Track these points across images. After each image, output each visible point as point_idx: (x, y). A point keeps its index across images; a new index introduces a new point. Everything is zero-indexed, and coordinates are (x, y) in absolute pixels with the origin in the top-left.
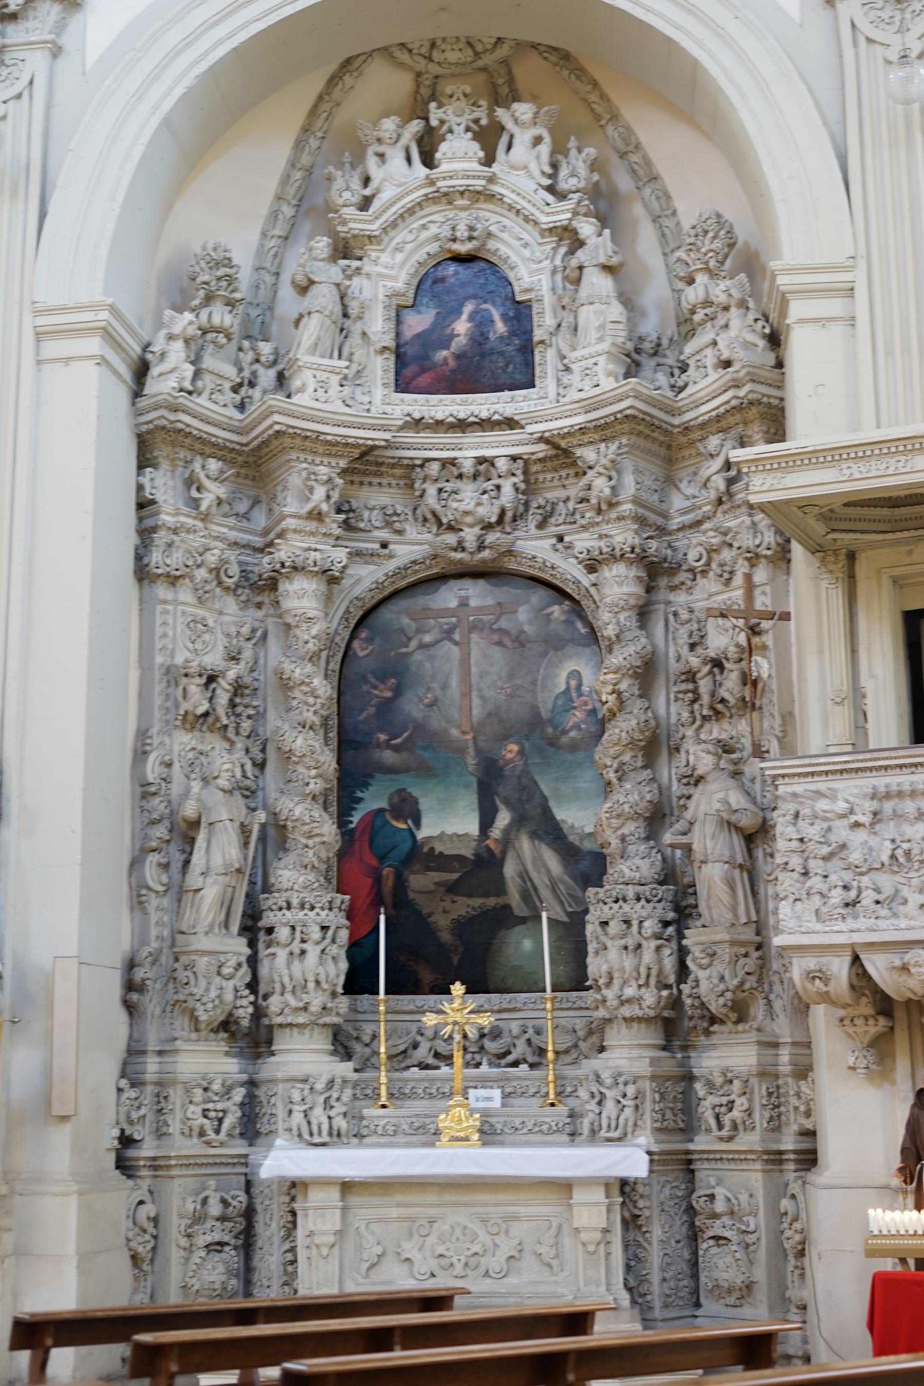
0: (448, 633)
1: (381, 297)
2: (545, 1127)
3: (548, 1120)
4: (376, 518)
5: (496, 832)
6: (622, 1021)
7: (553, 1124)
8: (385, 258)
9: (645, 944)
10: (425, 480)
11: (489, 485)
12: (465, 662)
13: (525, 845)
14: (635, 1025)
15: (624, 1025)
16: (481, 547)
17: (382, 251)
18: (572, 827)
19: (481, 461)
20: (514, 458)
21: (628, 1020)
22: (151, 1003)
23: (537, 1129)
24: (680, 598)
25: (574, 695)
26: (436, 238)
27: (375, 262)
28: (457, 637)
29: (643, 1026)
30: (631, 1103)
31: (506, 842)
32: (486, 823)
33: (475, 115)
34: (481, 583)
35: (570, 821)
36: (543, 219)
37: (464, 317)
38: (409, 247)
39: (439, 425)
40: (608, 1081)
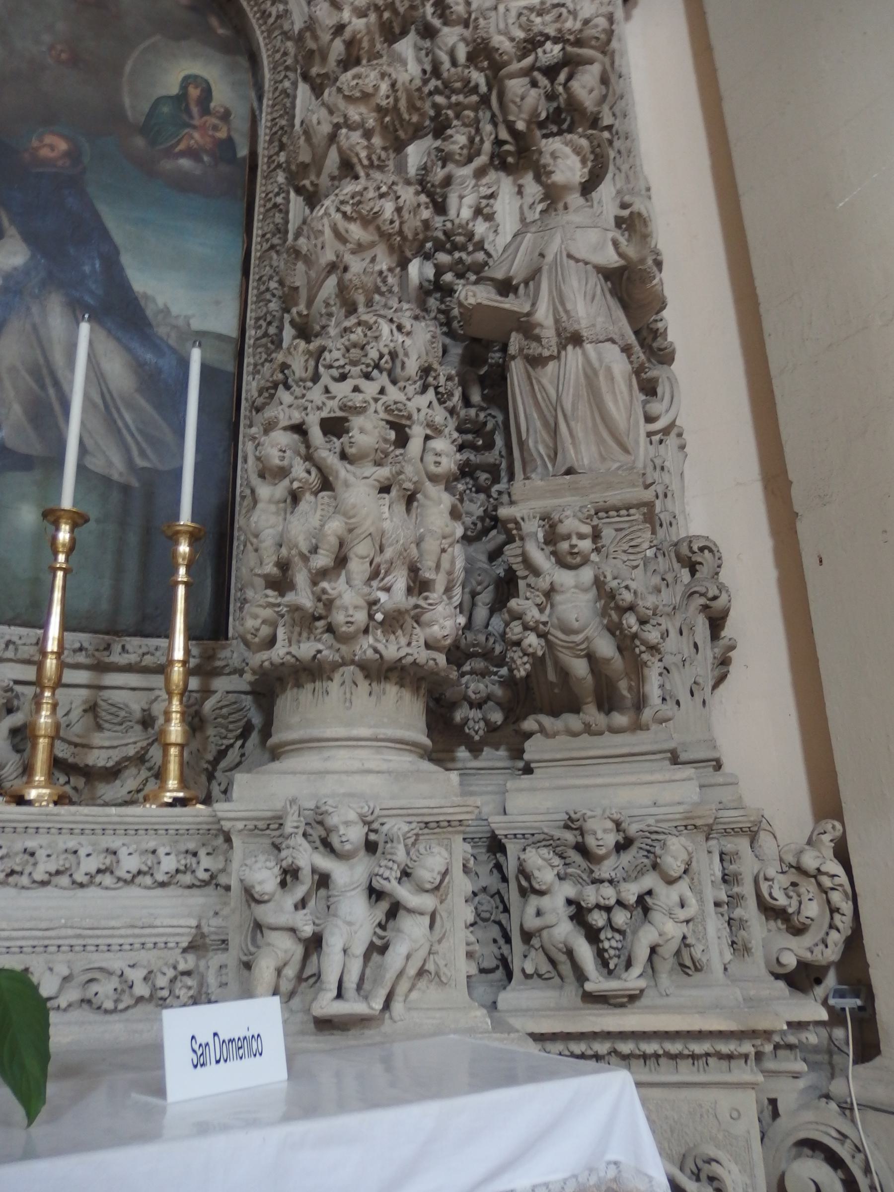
2: (105, 989)
3: (116, 963)
6: (359, 676)
7: (136, 976)
14: (392, 690)
15: (364, 685)
18: (166, 311)
23: (73, 994)
25: (195, 110)
30: (427, 902)
35: (160, 302)
40: (355, 835)
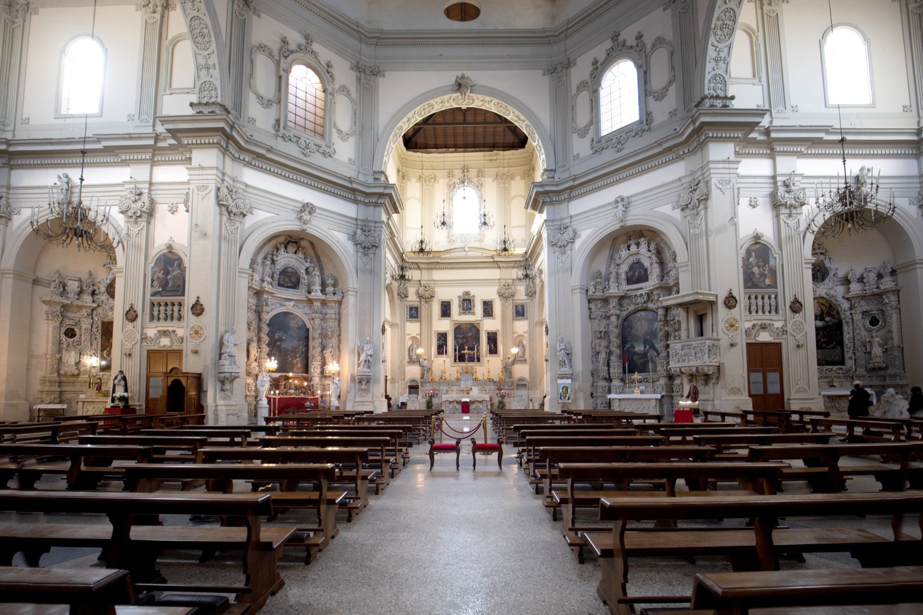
0: (638, 320)
4: (625, 304)
5: (646, 349)
12: (641, 324)
13: (651, 351)
22: (595, 376)
24: (672, 312)
31: (648, 351)
32: (645, 348)
39: (634, 290)
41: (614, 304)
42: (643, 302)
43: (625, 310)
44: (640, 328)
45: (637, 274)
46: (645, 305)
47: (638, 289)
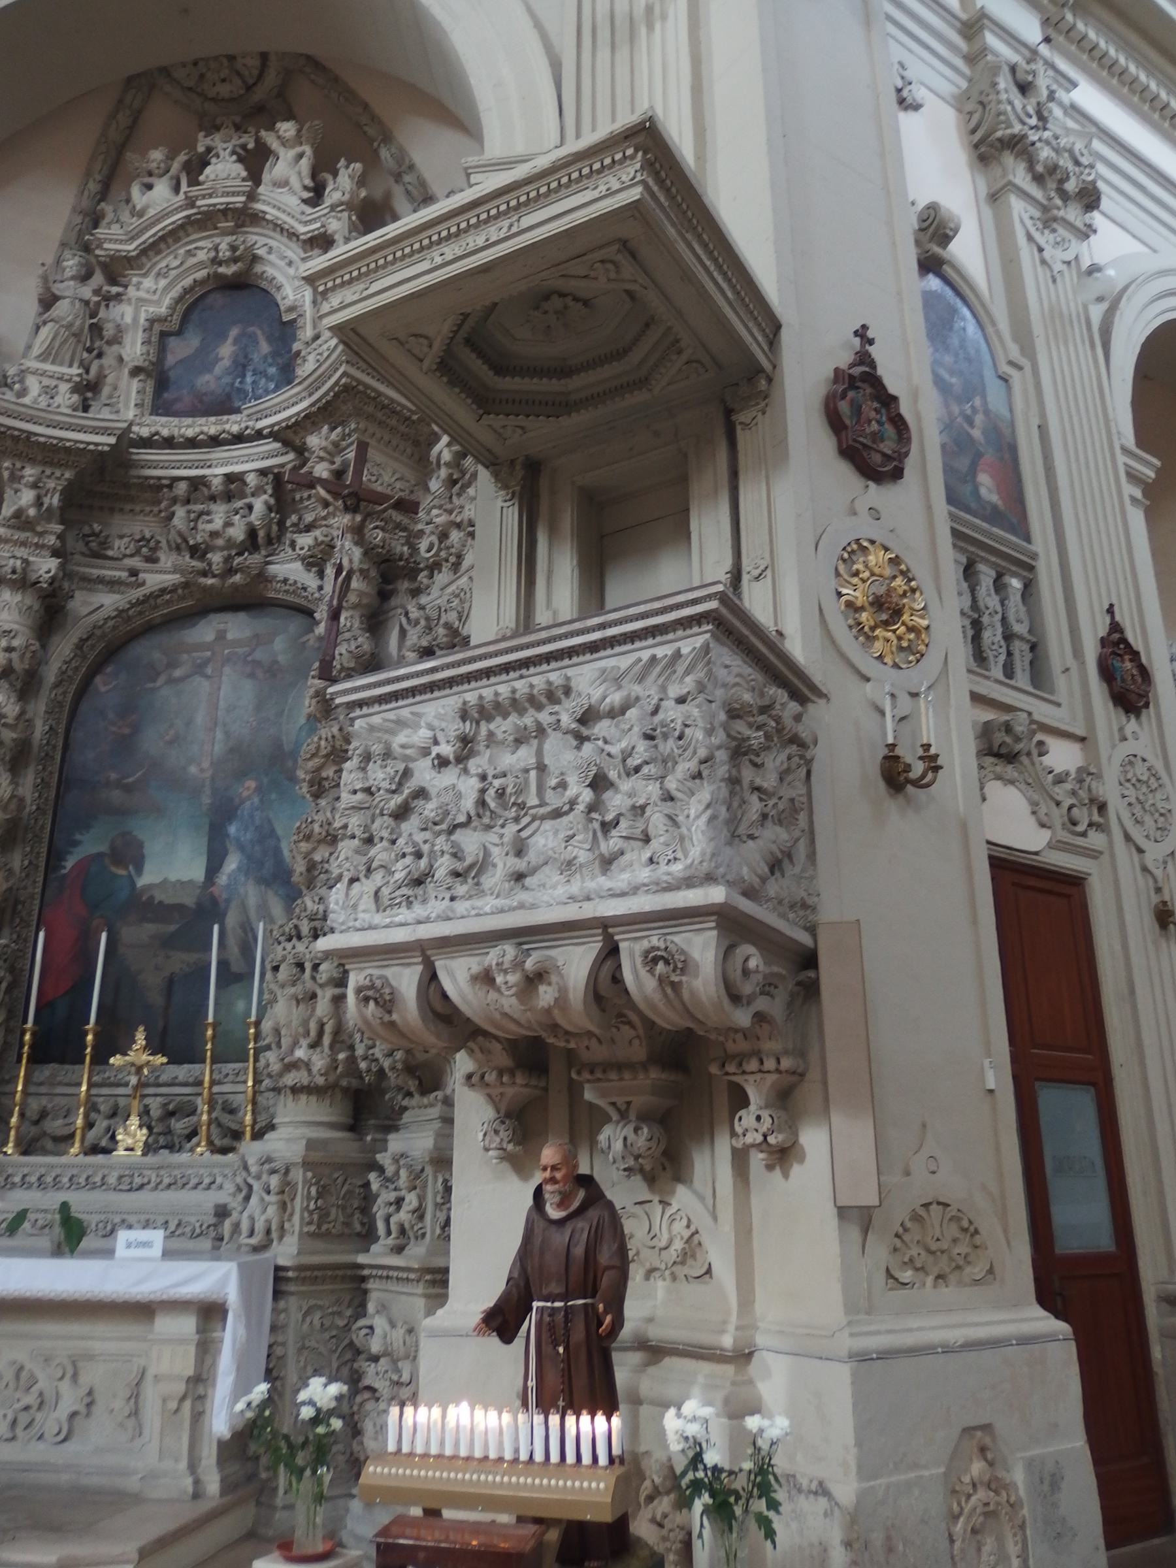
1: (142, 321)
8: (148, 283)
9: (319, 992)
10: (174, 501)
11: (239, 504)
14: (303, 1098)
15: (291, 1097)
16: (230, 571)
17: (145, 275)
19: (230, 478)
20: (263, 472)
21: (296, 1090)
26: (200, 265)
27: (138, 286)
28: (209, 671)
29: (313, 1099)
33: (242, 140)
34: (242, 616)
36: (302, 229)
37: (230, 340)
38: (173, 273)
41: (27, 497)
42: (238, 532)
43: (113, 585)
44: (200, 718)
45: (226, 351)
46: (254, 560)
47: (215, 441)
